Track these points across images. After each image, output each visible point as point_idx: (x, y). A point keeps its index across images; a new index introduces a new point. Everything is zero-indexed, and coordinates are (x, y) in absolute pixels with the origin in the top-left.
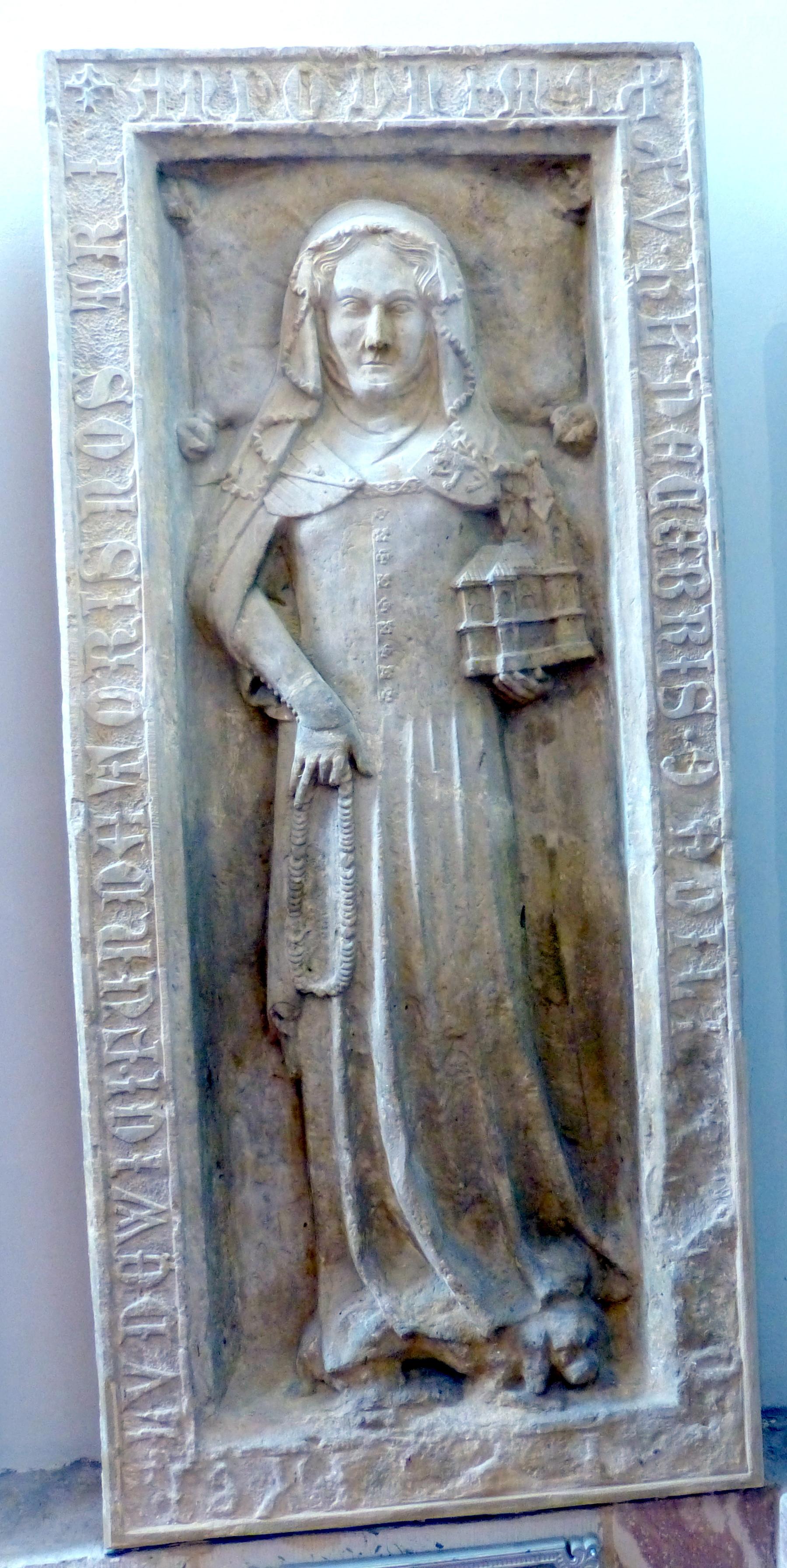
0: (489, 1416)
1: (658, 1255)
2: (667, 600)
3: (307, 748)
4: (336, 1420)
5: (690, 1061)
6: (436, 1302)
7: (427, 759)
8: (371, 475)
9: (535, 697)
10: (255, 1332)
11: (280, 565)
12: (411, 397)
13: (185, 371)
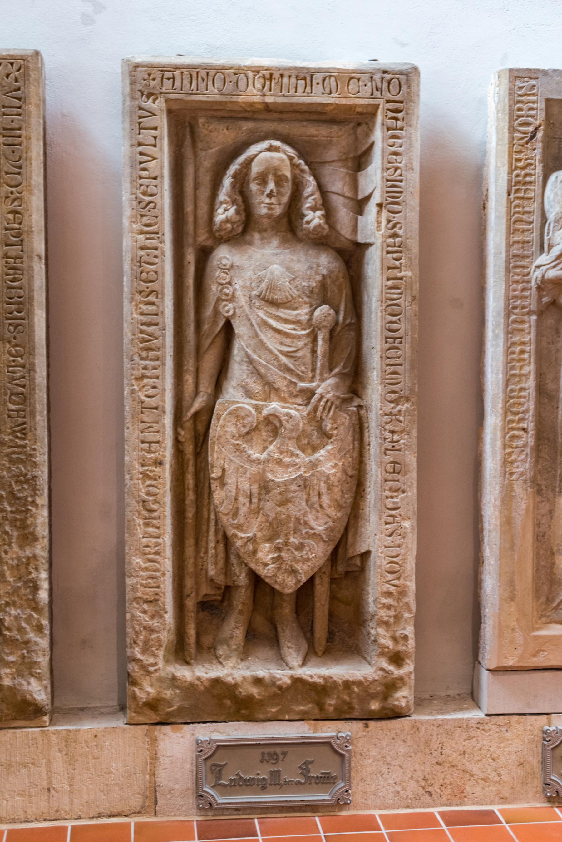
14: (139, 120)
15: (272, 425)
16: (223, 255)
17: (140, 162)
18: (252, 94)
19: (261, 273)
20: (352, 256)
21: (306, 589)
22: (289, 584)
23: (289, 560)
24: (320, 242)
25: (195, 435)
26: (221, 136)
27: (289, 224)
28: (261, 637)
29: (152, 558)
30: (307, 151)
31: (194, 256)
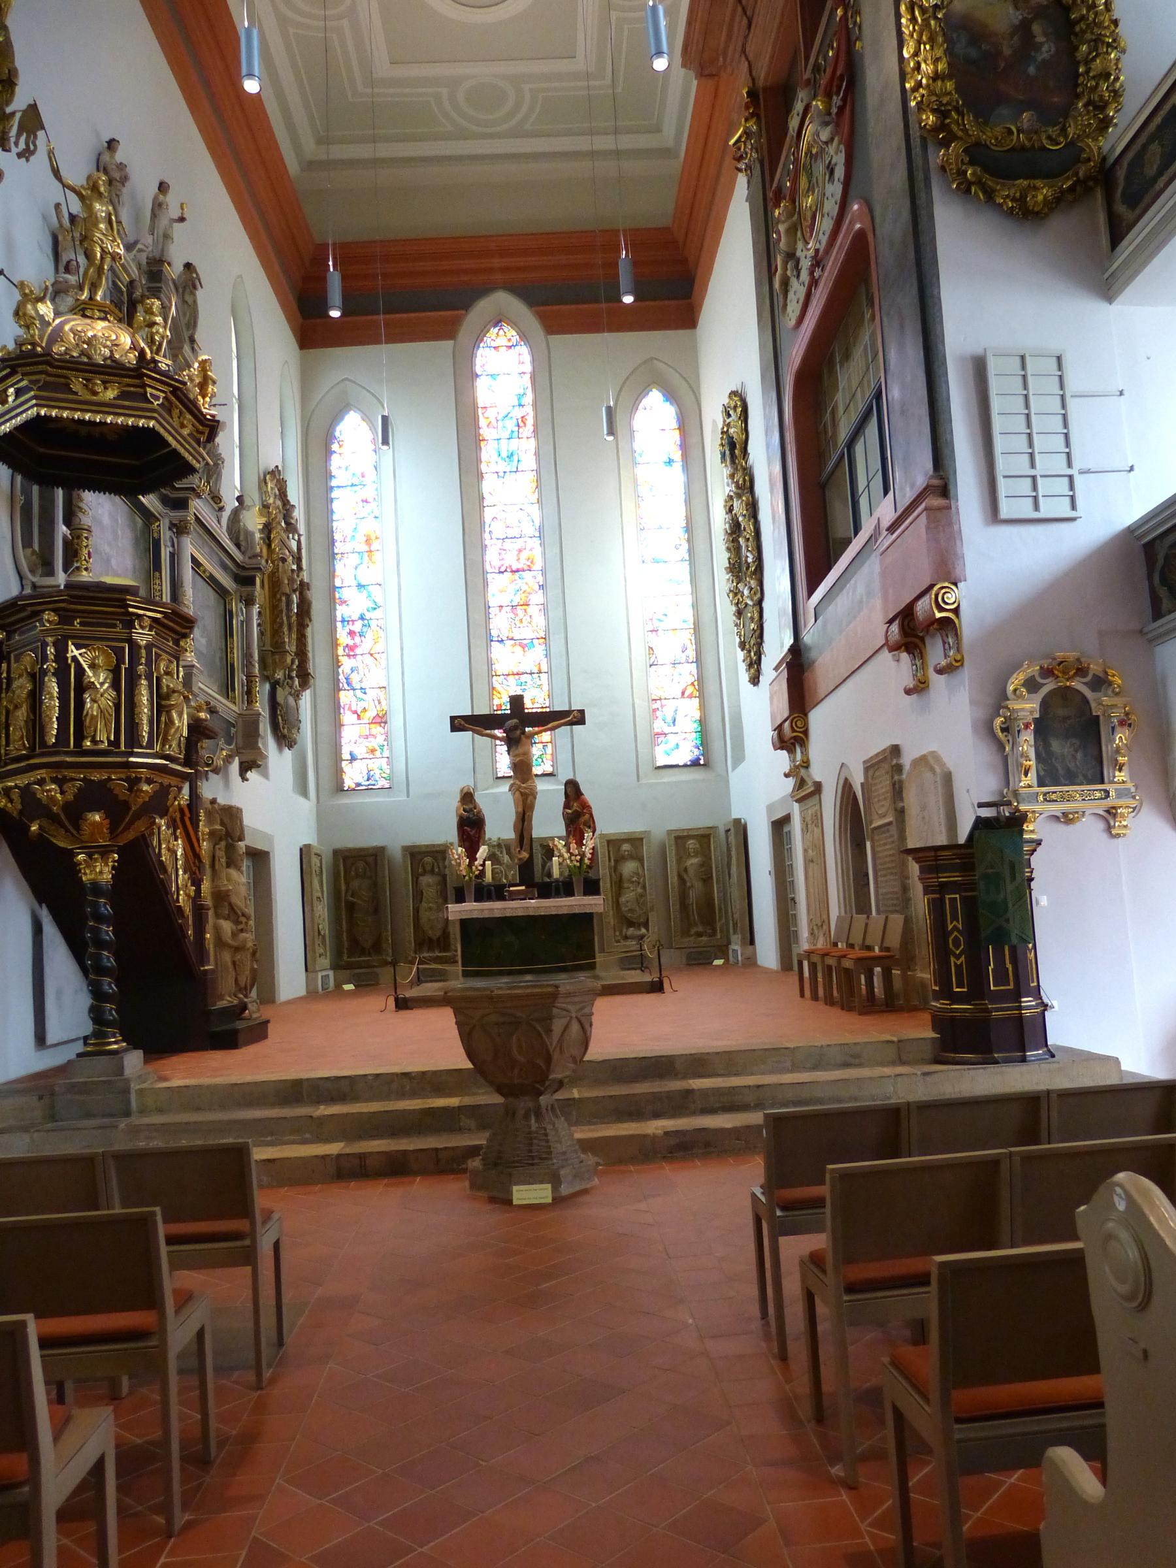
0: (704, 938)
1: (718, 925)
2: (717, 872)
3: (688, 884)
4: (692, 939)
5: (720, 909)
6: (700, 929)
7: (698, 885)
8: (694, 861)
9: (707, 880)
10: (686, 933)
11: (686, 870)
12: (696, 856)
13: (677, 853)
14: (404, 856)
15: (430, 909)
16: (421, 878)
17: (404, 861)
18: (424, 849)
19: (427, 880)
20: (444, 877)
21: (438, 939)
22: (435, 938)
23: (436, 934)
24: (439, 874)
25: (417, 911)
26: (419, 857)
27: (432, 872)
28: (430, 949)
29: (409, 933)
30: (435, 858)
31: (416, 878)
